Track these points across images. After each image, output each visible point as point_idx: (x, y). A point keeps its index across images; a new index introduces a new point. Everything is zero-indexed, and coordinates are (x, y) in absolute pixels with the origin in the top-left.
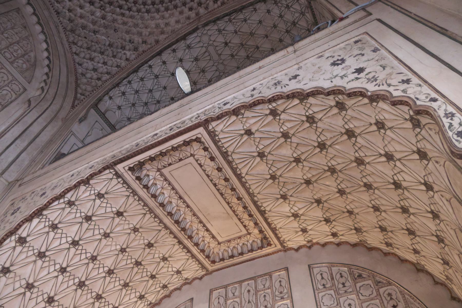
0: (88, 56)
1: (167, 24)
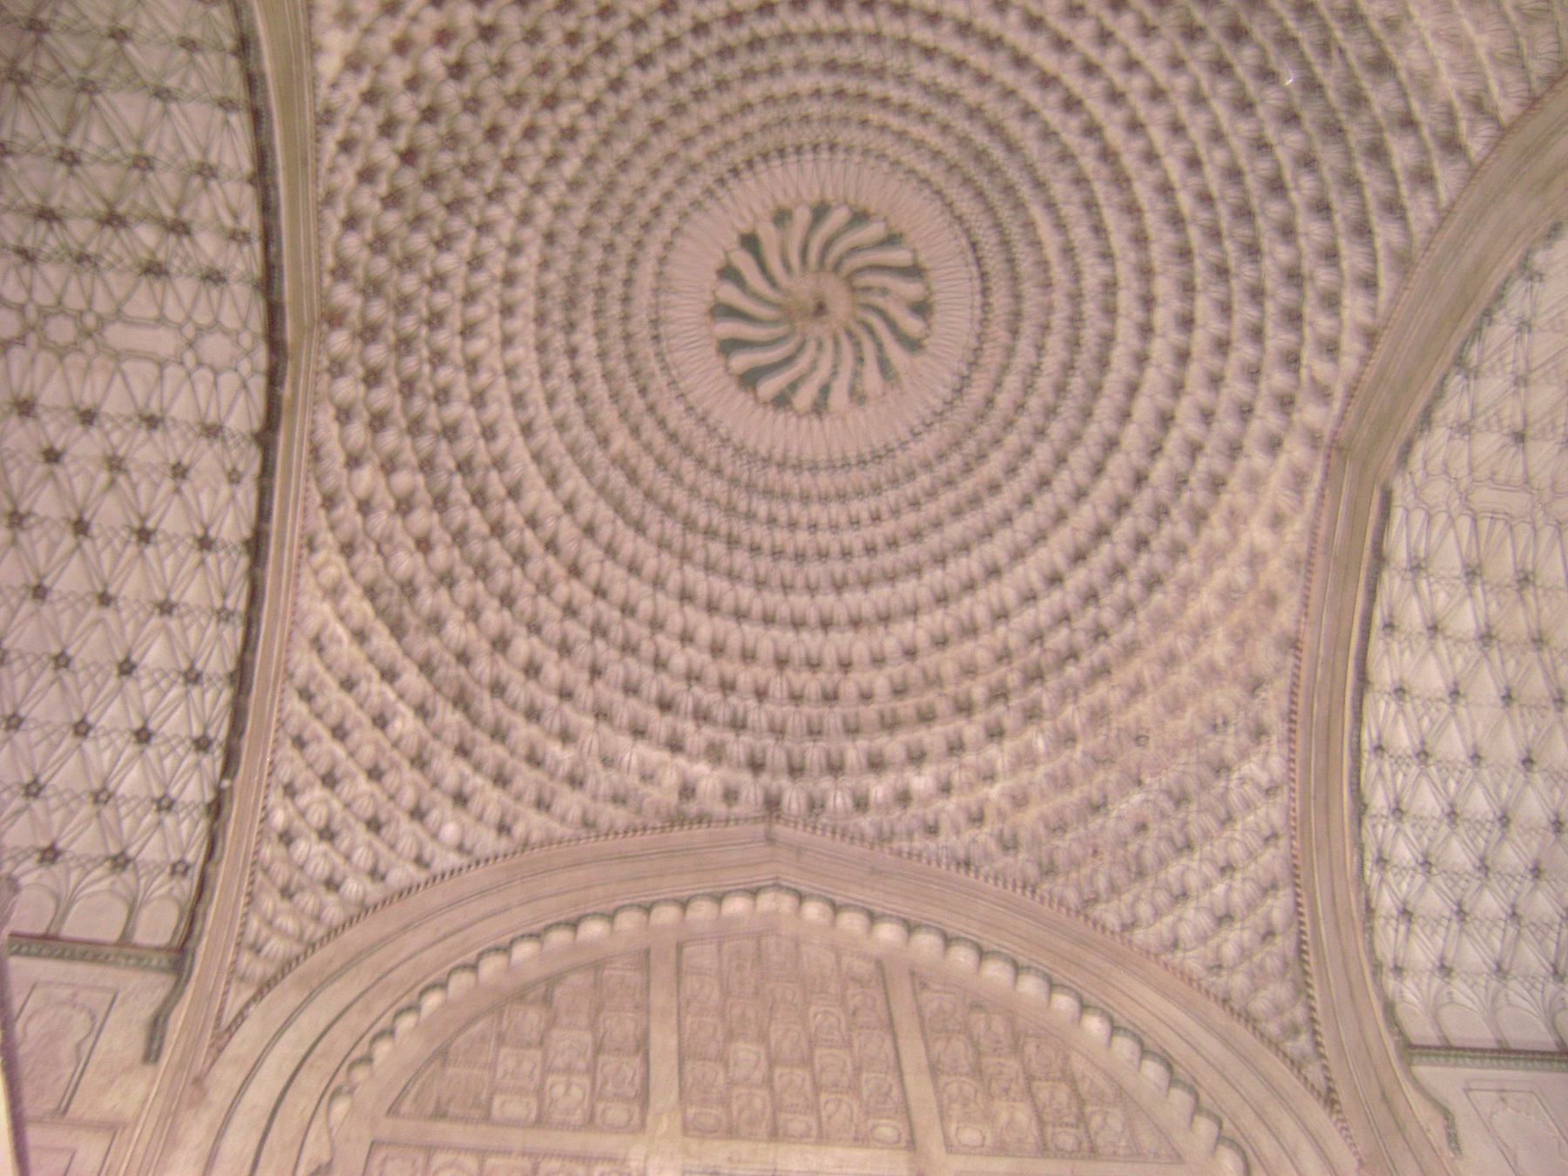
0: (1162, 898)
1: (1255, 560)
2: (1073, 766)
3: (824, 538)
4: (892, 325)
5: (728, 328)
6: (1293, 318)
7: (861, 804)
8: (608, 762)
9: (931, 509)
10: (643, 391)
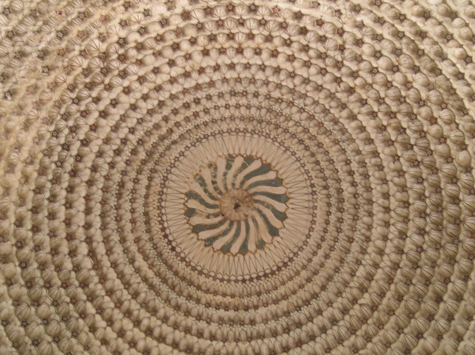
4: (202, 202)
5: (279, 190)
6: (30, 284)
10: (317, 163)
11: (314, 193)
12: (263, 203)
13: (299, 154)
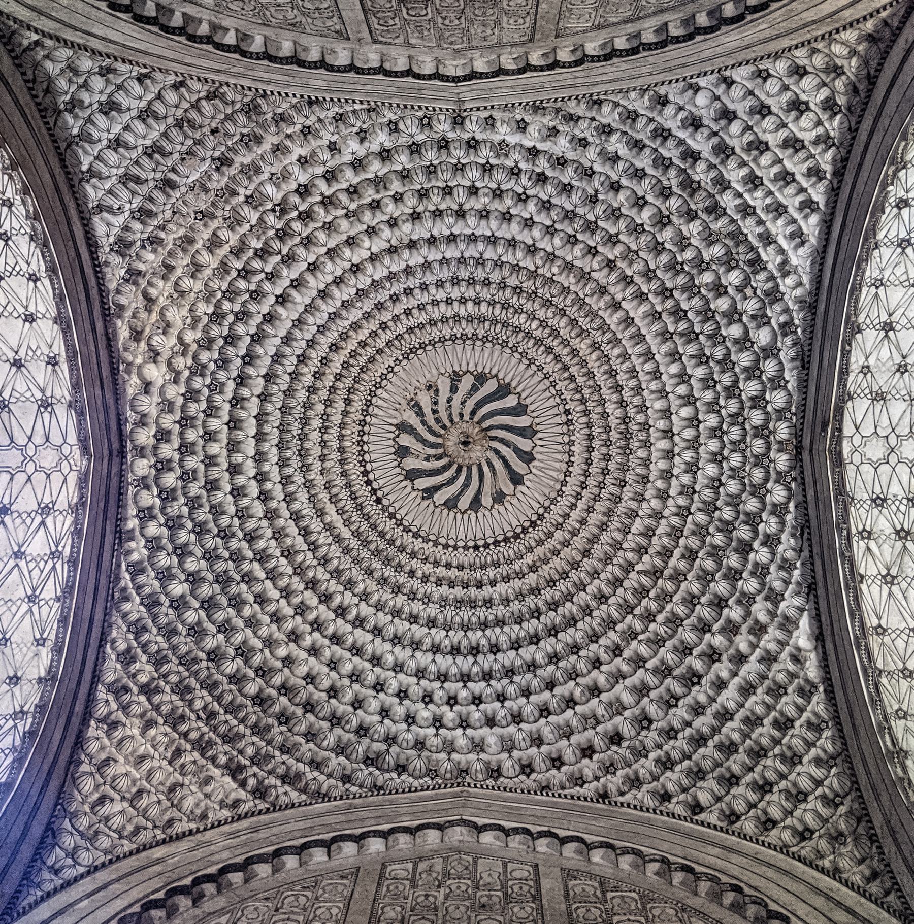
2: (246, 183)
3: (441, 295)
5: (523, 422)
7: (393, 128)
8: (583, 143)
9: (373, 325)
10: (572, 378)
11: (569, 422)
12: (502, 441)
13: (548, 369)
